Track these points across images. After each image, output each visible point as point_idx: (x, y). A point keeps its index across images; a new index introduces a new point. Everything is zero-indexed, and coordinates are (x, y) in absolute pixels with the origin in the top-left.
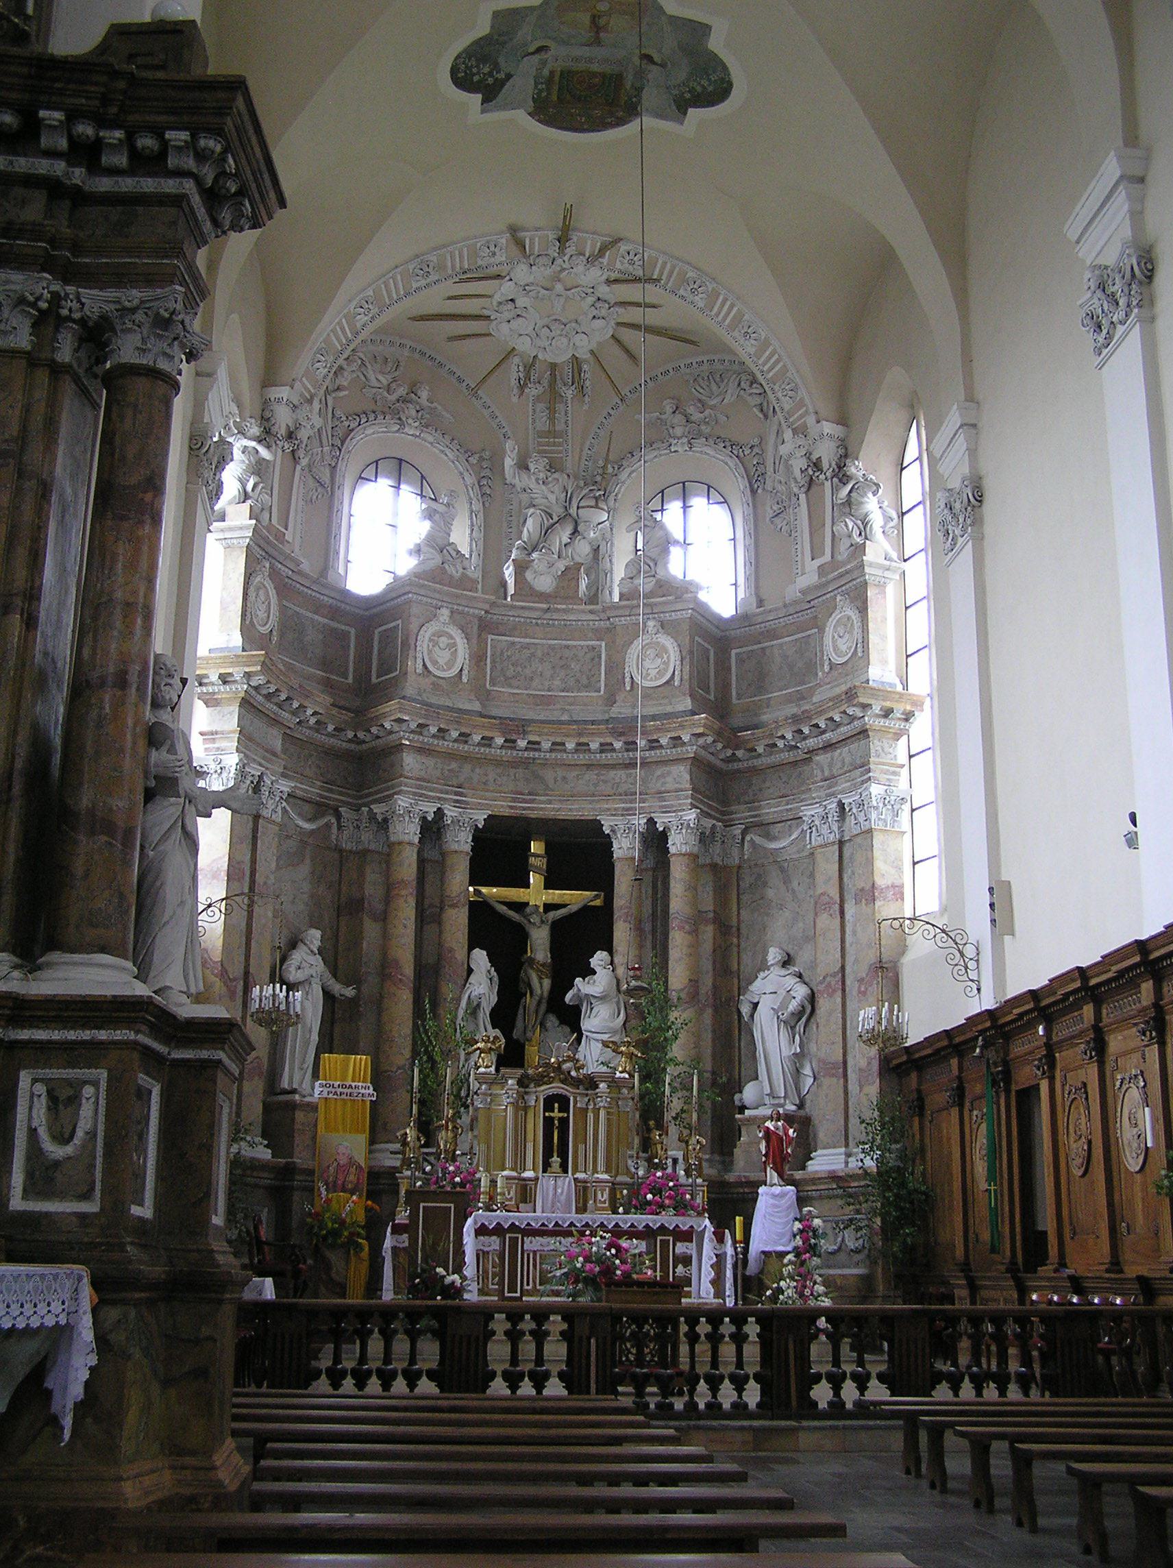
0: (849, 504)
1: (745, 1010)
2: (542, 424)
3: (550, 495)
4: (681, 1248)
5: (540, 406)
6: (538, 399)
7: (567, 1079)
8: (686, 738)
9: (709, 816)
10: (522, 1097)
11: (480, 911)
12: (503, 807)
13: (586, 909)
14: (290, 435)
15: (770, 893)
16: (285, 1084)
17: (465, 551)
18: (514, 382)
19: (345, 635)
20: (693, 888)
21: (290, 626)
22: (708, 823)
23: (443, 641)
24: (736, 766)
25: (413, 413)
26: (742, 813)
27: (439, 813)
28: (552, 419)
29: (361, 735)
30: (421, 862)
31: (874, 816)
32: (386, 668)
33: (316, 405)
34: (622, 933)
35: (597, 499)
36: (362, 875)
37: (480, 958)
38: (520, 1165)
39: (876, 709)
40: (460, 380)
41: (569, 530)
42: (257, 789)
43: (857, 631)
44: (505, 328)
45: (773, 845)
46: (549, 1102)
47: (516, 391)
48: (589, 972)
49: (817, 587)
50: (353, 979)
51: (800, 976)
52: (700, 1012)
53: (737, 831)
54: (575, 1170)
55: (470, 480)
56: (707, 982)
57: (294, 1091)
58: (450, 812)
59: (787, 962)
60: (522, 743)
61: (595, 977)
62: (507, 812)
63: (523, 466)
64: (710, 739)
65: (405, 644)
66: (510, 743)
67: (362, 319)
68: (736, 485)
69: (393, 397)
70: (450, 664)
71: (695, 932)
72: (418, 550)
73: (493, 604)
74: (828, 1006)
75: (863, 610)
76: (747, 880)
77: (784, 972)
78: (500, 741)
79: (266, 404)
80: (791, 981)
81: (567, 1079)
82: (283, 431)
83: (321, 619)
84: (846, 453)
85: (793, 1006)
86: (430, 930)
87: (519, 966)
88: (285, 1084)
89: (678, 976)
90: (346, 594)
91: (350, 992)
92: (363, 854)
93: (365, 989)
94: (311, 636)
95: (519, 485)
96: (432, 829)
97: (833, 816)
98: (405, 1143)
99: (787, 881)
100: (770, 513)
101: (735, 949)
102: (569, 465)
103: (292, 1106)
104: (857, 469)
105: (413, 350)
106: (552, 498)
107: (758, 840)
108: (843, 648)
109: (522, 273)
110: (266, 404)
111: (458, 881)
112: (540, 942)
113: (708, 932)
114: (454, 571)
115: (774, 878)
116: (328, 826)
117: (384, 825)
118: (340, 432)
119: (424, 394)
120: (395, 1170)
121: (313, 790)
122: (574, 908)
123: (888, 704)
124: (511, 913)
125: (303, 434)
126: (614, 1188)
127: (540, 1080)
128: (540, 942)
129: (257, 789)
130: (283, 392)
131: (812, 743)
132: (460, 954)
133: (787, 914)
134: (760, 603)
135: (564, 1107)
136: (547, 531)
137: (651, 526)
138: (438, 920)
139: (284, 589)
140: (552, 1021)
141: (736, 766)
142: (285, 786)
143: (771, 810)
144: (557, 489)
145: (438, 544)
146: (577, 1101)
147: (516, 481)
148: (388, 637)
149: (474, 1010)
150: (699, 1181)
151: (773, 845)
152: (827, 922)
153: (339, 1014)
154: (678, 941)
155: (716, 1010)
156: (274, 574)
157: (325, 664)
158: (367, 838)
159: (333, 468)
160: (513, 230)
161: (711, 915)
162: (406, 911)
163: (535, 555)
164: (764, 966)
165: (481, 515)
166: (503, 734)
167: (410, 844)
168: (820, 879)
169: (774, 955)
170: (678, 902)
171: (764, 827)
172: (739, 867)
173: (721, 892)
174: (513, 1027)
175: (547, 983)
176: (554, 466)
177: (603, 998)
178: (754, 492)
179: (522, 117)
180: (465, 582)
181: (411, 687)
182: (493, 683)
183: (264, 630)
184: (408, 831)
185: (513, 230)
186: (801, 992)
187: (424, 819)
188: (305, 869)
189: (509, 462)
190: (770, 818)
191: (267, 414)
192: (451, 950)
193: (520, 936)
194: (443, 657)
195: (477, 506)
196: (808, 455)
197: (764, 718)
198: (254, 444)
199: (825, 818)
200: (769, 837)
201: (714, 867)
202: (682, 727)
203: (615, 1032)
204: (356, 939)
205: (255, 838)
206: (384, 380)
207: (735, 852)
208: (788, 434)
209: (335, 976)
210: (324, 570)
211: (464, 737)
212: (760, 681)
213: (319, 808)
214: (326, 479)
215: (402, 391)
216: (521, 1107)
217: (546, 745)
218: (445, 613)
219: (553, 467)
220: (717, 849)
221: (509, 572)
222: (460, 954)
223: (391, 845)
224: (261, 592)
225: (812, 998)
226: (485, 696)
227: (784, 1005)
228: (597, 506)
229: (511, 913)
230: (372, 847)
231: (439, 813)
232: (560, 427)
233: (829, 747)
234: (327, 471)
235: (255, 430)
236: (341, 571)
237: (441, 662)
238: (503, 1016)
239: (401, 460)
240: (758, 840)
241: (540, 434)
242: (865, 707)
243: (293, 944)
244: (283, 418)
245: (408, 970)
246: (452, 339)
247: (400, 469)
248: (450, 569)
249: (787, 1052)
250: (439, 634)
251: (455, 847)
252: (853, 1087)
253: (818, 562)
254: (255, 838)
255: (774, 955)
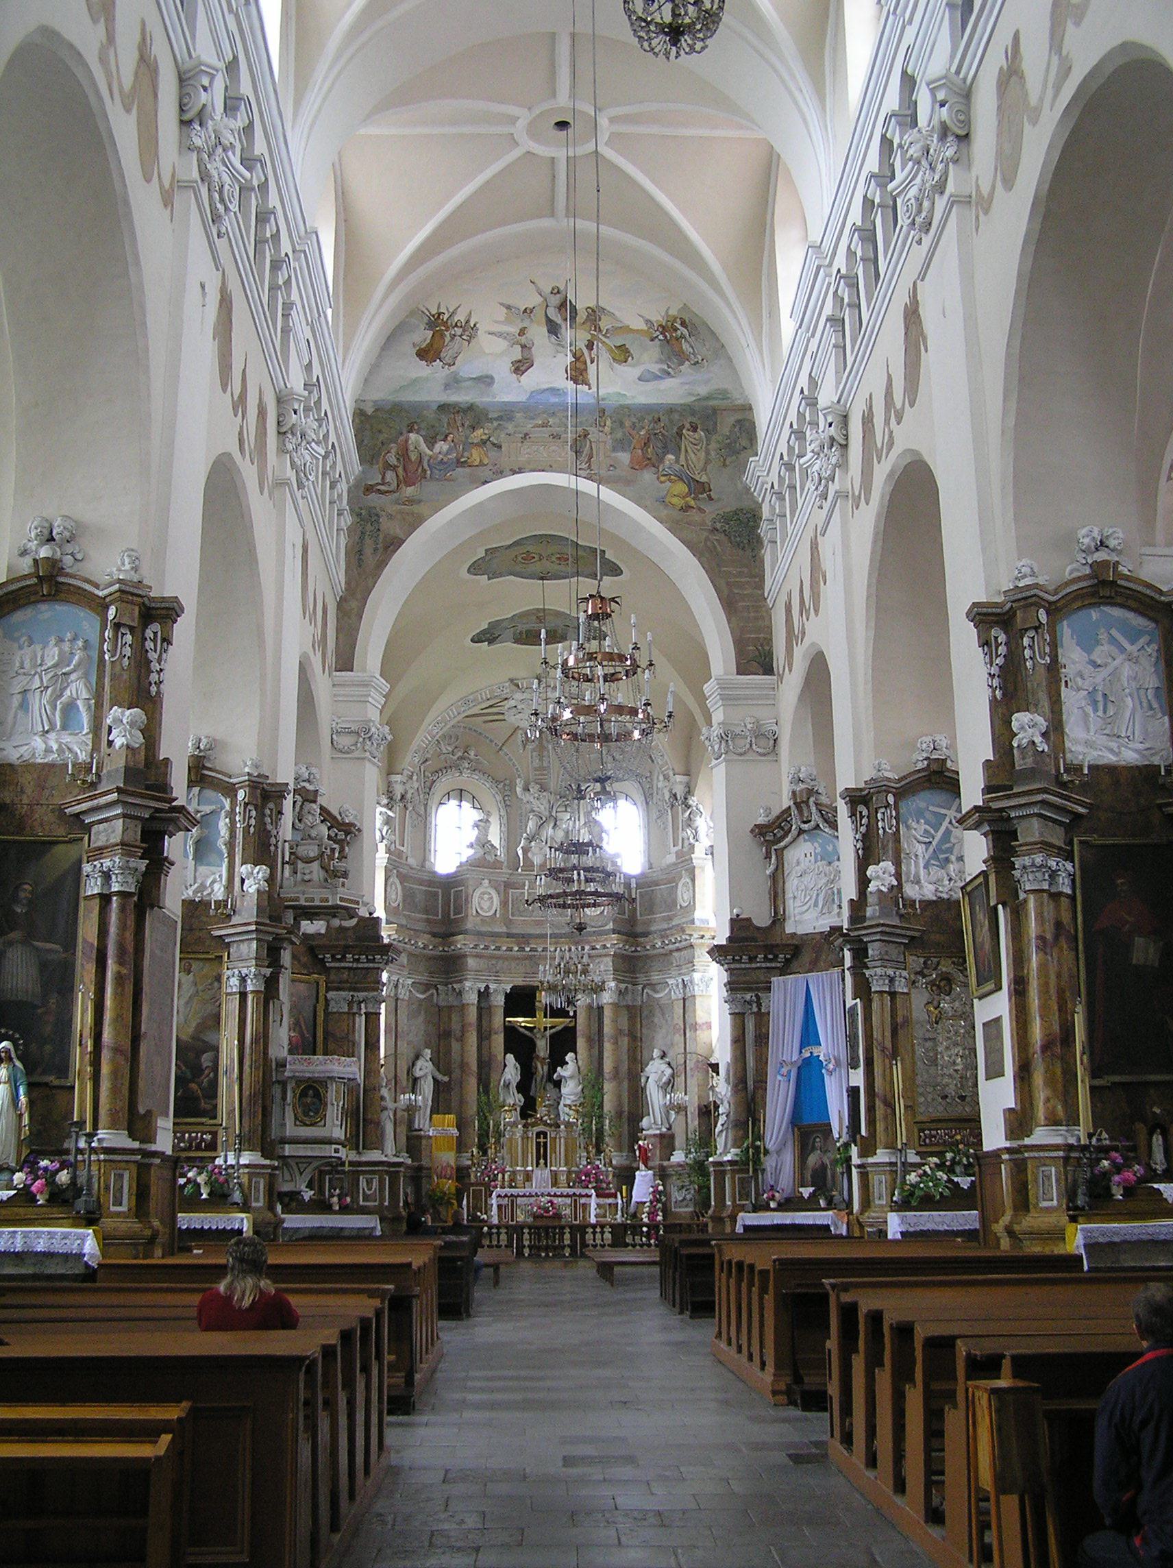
0: (689, 822)
1: (643, 1080)
2: (536, 763)
3: (542, 807)
4: (583, 1200)
5: (534, 754)
6: (533, 750)
7: (546, 1124)
8: (608, 946)
9: (624, 982)
10: (525, 1132)
11: (510, 1031)
12: (519, 981)
13: (566, 1029)
14: (403, 797)
15: (656, 1020)
16: (416, 1126)
17: (498, 847)
18: (520, 743)
19: (436, 894)
20: (615, 1021)
21: (408, 897)
22: (623, 986)
23: (486, 897)
24: (637, 954)
25: (467, 765)
26: (642, 979)
27: (487, 987)
28: (541, 760)
29: (446, 949)
30: (479, 1008)
31: (696, 988)
32: (457, 912)
33: (415, 777)
34: (581, 1043)
35: (566, 806)
36: (450, 1018)
37: (510, 1057)
38: (525, 1164)
39: (696, 936)
40: (491, 741)
41: (552, 825)
42: (396, 986)
43: (691, 891)
44: (513, 718)
45: (657, 996)
46: (538, 1135)
47: (521, 747)
48: (564, 1063)
49: (675, 864)
50: (448, 1072)
51: (669, 1064)
52: (620, 1084)
53: (640, 987)
54: (551, 1166)
55: (499, 798)
56: (624, 1068)
57: (421, 1130)
58: (492, 987)
59: (663, 1056)
60: (528, 949)
61: (568, 1066)
62: (521, 984)
63: (526, 789)
64: (621, 946)
65: (466, 900)
66: (520, 950)
67: (434, 733)
68: (640, 798)
69: (455, 758)
70: (490, 908)
71: (616, 1043)
72: (471, 846)
73: (511, 874)
74: (680, 1081)
75: (693, 880)
76: (645, 1013)
77: (661, 1061)
78: (516, 949)
79: (389, 784)
80: (664, 1067)
81: (546, 1124)
82: (399, 798)
83: (424, 888)
84: (689, 792)
85: (664, 1079)
86: (485, 1043)
87: (532, 1059)
88: (416, 1126)
89: (608, 1066)
90: (435, 873)
91: (446, 1079)
92: (451, 1007)
93: (453, 1076)
94: (419, 898)
95: (525, 800)
96: (484, 995)
97: (681, 986)
98: (472, 1155)
99: (663, 1014)
100: (655, 817)
101: (639, 1048)
102: (552, 786)
103: (420, 1137)
104: (693, 801)
105: (465, 728)
106: (542, 807)
107: (651, 993)
108: (686, 898)
109: (519, 696)
110: (389, 784)
111: (498, 1020)
112: (542, 1048)
113: (625, 1041)
114: (490, 858)
115: (657, 1012)
116: (432, 995)
117: (460, 993)
118: (428, 784)
119: (472, 753)
120: (469, 1167)
121: (423, 978)
122: (559, 1028)
123: (702, 933)
124: (527, 1032)
125: (409, 796)
126: (569, 1173)
127: (533, 1125)
128: (542, 1048)
129: (396, 986)
130: (398, 778)
131: (671, 947)
132: (500, 1057)
133: (664, 1031)
134: (651, 868)
135: (545, 1137)
136: (540, 827)
137: (592, 824)
138: (489, 1037)
139: (403, 878)
140: (550, 1086)
141: (637, 954)
142: (410, 982)
143: (656, 977)
144: (545, 802)
145: (483, 843)
146: (551, 1133)
147: (523, 797)
148: (458, 895)
149: (507, 1086)
150: (610, 1169)
151: (657, 996)
152: (679, 1038)
153: (441, 1089)
154: (608, 1046)
155: (630, 1080)
156: (399, 875)
157: (426, 912)
158: (452, 1000)
159: (426, 805)
160: (511, 680)
161: (626, 1032)
162: (472, 1038)
163: (533, 844)
164: (652, 1059)
165: (505, 818)
166: (518, 945)
167: (473, 1004)
168: (676, 1017)
169: (656, 1053)
170: (608, 1029)
171: (652, 986)
172: (641, 1007)
173: (632, 1018)
174: (529, 1090)
175: (546, 1068)
176: (543, 788)
177: (571, 1077)
178: (647, 803)
179: (510, 645)
180: (496, 865)
181: (469, 925)
182: (513, 915)
183: (395, 905)
184: (472, 998)
185: (511, 680)
186: (669, 1071)
187: (479, 991)
188: (421, 1018)
189: (518, 790)
190: (654, 982)
191: (391, 789)
192: (496, 1056)
193: (532, 1044)
194: (486, 905)
195: (503, 812)
196: (670, 791)
197: (653, 929)
198: (384, 810)
199: (677, 985)
200: (656, 992)
201: (628, 1007)
202: (606, 939)
203: (575, 1094)
204: (449, 1052)
205: (396, 1010)
206: (450, 749)
207: (639, 999)
208: (661, 778)
209: (439, 1070)
210: (425, 859)
211: (498, 948)
212: (650, 908)
213: (427, 987)
214: (422, 812)
215: (460, 754)
216: (525, 1138)
217: (540, 949)
218: (486, 881)
219: (543, 788)
220: (629, 997)
221: (520, 852)
222: (500, 1057)
223: (463, 1005)
224: (394, 888)
225: (673, 1076)
226: (508, 923)
227: (660, 1079)
228: (566, 811)
229: (527, 1032)
230: (455, 1003)
231: (487, 987)
232: (545, 765)
233: (678, 950)
234: (423, 808)
235: (385, 801)
236: (432, 860)
237: (486, 908)
238: (523, 1087)
239: (461, 790)
240: (651, 993)
241: (536, 769)
242: (691, 935)
243: (417, 1057)
244: (398, 790)
245: (474, 1067)
246: (485, 722)
247: (461, 794)
248: (487, 857)
249: (662, 1103)
250: (484, 893)
251: (496, 1004)
252: (689, 1121)
253: (676, 849)
254: (396, 1010)
255: (656, 1053)
